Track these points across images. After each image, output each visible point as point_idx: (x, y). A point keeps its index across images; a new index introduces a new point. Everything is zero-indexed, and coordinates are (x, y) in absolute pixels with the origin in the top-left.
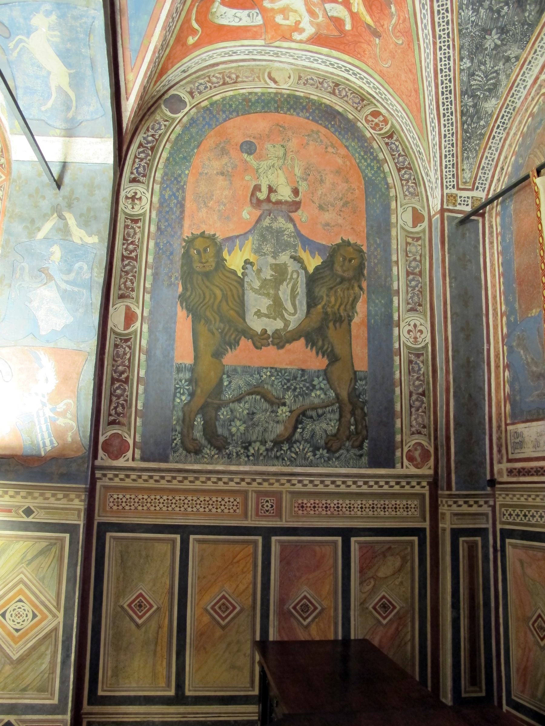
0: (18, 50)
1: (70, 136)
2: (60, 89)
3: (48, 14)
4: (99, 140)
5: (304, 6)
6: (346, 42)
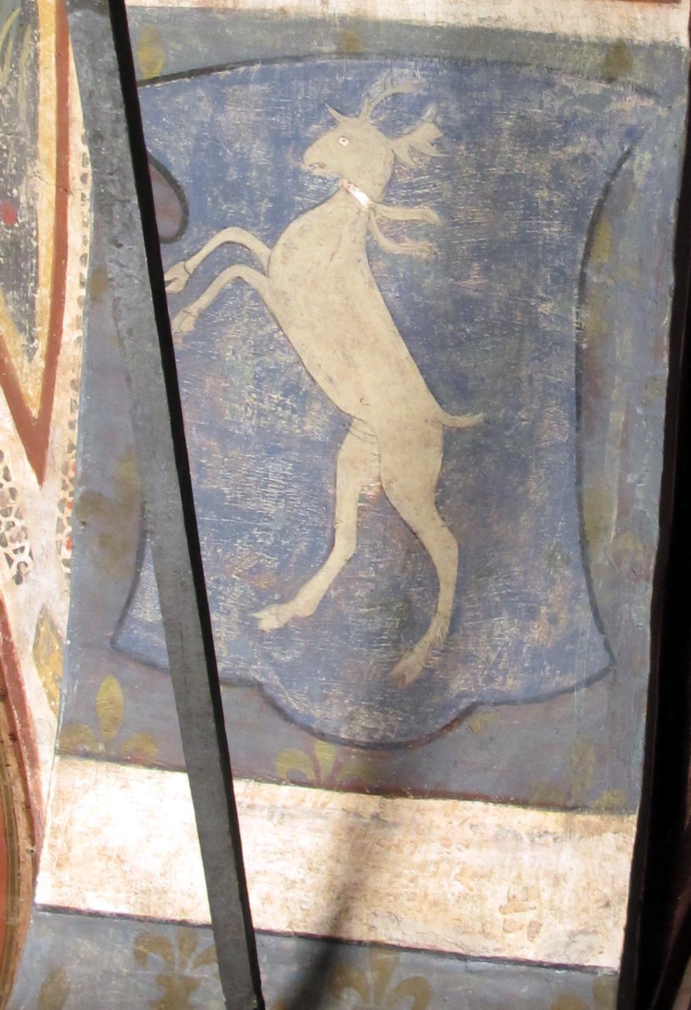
0: (205, 300)
1: (388, 787)
2: (380, 510)
3: (396, 118)
4: (552, 820)
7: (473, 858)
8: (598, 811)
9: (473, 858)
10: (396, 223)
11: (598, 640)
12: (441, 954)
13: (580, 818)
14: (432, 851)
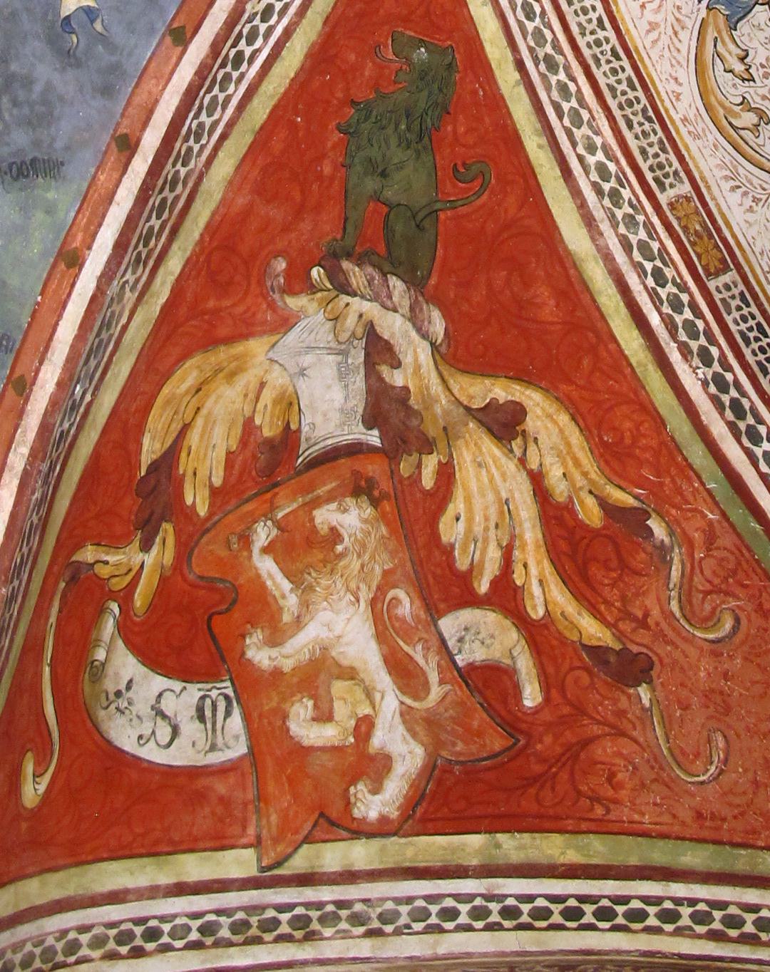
6: (537, 768)
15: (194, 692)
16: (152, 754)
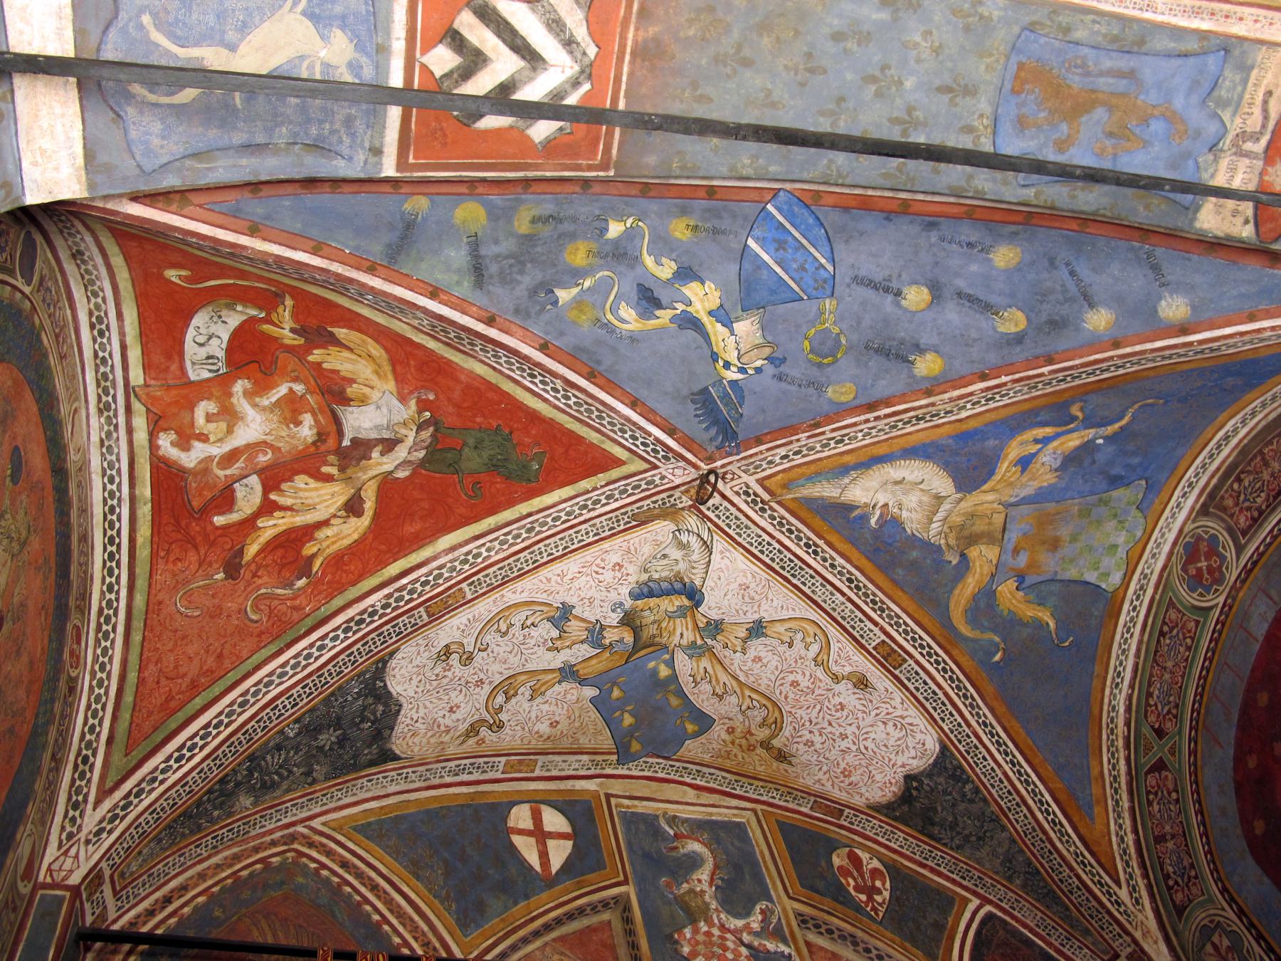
3: (353, 66)
4: (80, 161)
5: (244, 442)
6: (183, 523)
7: (59, 129)
8: (88, 179)
9: (59, 129)
10: (314, 67)
11: (156, 167)
12: (16, 124)
13: (83, 172)
14: (58, 110)
15: (221, 354)
16: (191, 333)
